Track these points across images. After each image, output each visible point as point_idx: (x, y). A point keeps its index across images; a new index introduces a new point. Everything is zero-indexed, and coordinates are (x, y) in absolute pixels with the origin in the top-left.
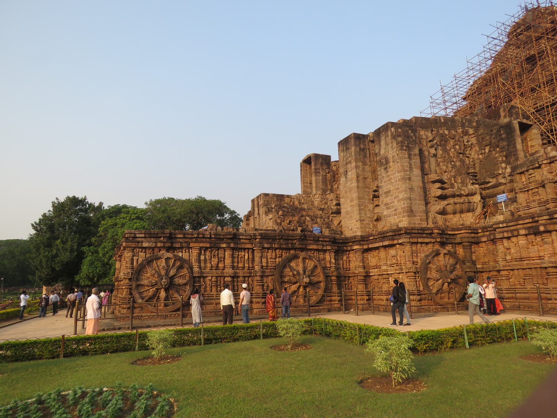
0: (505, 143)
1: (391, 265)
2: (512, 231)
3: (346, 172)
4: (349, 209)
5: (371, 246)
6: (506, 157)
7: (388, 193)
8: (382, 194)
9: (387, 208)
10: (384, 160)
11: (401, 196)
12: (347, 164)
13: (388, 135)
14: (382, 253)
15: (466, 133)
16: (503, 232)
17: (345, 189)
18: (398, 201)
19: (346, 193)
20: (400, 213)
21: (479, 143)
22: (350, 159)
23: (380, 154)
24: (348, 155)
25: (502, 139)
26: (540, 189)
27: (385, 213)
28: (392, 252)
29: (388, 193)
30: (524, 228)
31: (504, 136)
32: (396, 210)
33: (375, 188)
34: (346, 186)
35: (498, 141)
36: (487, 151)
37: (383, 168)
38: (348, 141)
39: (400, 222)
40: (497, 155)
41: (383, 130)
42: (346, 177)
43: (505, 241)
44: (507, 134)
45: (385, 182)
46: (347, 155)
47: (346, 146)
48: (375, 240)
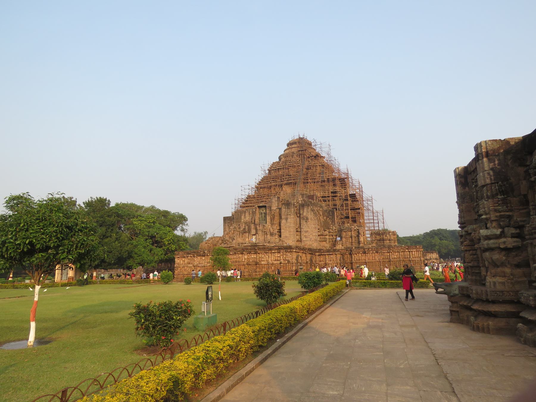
0: (331, 217)
1: (330, 261)
2: (358, 252)
3: (287, 219)
4: (288, 235)
5: (322, 254)
6: (332, 222)
7: (307, 232)
8: (303, 231)
9: (305, 238)
10: (305, 218)
11: (314, 234)
12: (287, 215)
13: (309, 209)
14: (327, 256)
15: (320, 209)
16: (355, 252)
17: (285, 226)
18: (312, 236)
19: (285, 227)
20: (313, 241)
21: (323, 214)
22: (289, 214)
23: (303, 215)
24: (289, 211)
25: (330, 215)
26: (350, 238)
27: (304, 239)
28: (332, 256)
29: (307, 232)
30: (362, 252)
31: (331, 214)
32: (310, 239)
33: (297, 228)
34: (286, 225)
35: (329, 215)
36: (325, 218)
37: (304, 221)
38: (289, 205)
39: (313, 244)
40: (329, 221)
41: (306, 206)
42: (286, 221)
43: (355, 255)
44: (332, 214)
45: (306, 227)
46: (288, 211)
47: (288, 207)
48: (324, 252)
